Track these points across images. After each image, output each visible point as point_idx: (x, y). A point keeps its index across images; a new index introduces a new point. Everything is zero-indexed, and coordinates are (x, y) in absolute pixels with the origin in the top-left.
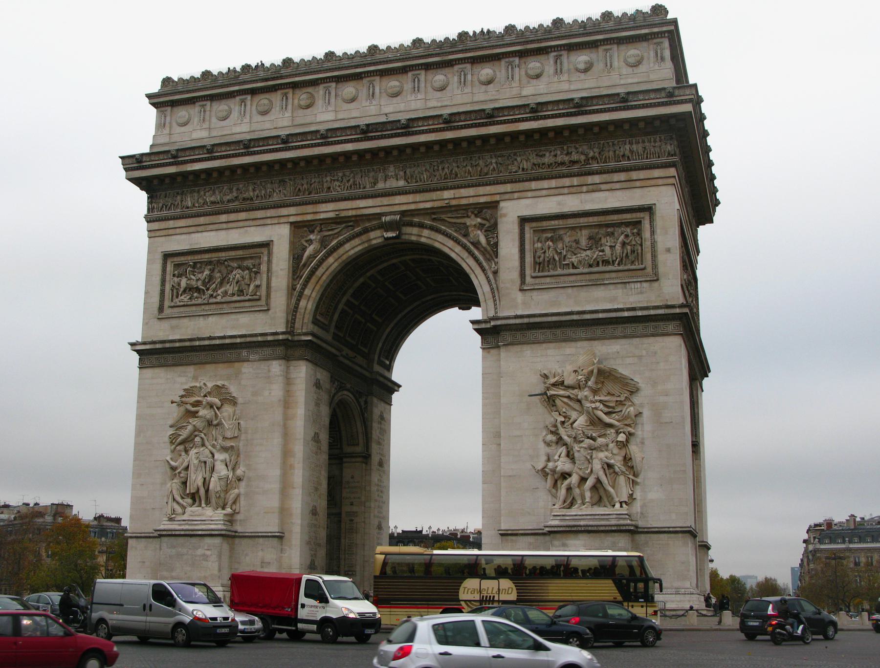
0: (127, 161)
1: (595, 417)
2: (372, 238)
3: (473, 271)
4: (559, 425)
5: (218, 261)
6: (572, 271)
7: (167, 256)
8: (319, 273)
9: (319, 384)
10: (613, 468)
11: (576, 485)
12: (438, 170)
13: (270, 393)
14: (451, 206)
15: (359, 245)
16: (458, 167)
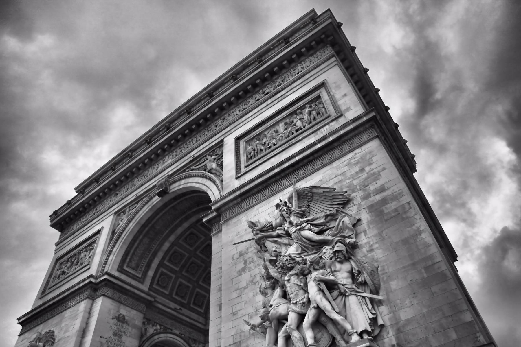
0: (53, 216)
1: (304, 240)
2: (154, 201)
3: (208, 188)
4: (268, 263)
5: (78, 252)
6: (273, 147)
7: (57, 260)
8: (123, 236)
9: (124, 319)
10: (339, 288)
11: (293, 326)
12: (190, 144)
13: (73, 327)
14: (196, 158)
15: (147, 208)
16: (200, 136)
